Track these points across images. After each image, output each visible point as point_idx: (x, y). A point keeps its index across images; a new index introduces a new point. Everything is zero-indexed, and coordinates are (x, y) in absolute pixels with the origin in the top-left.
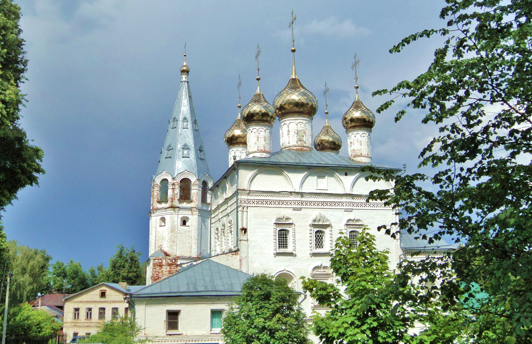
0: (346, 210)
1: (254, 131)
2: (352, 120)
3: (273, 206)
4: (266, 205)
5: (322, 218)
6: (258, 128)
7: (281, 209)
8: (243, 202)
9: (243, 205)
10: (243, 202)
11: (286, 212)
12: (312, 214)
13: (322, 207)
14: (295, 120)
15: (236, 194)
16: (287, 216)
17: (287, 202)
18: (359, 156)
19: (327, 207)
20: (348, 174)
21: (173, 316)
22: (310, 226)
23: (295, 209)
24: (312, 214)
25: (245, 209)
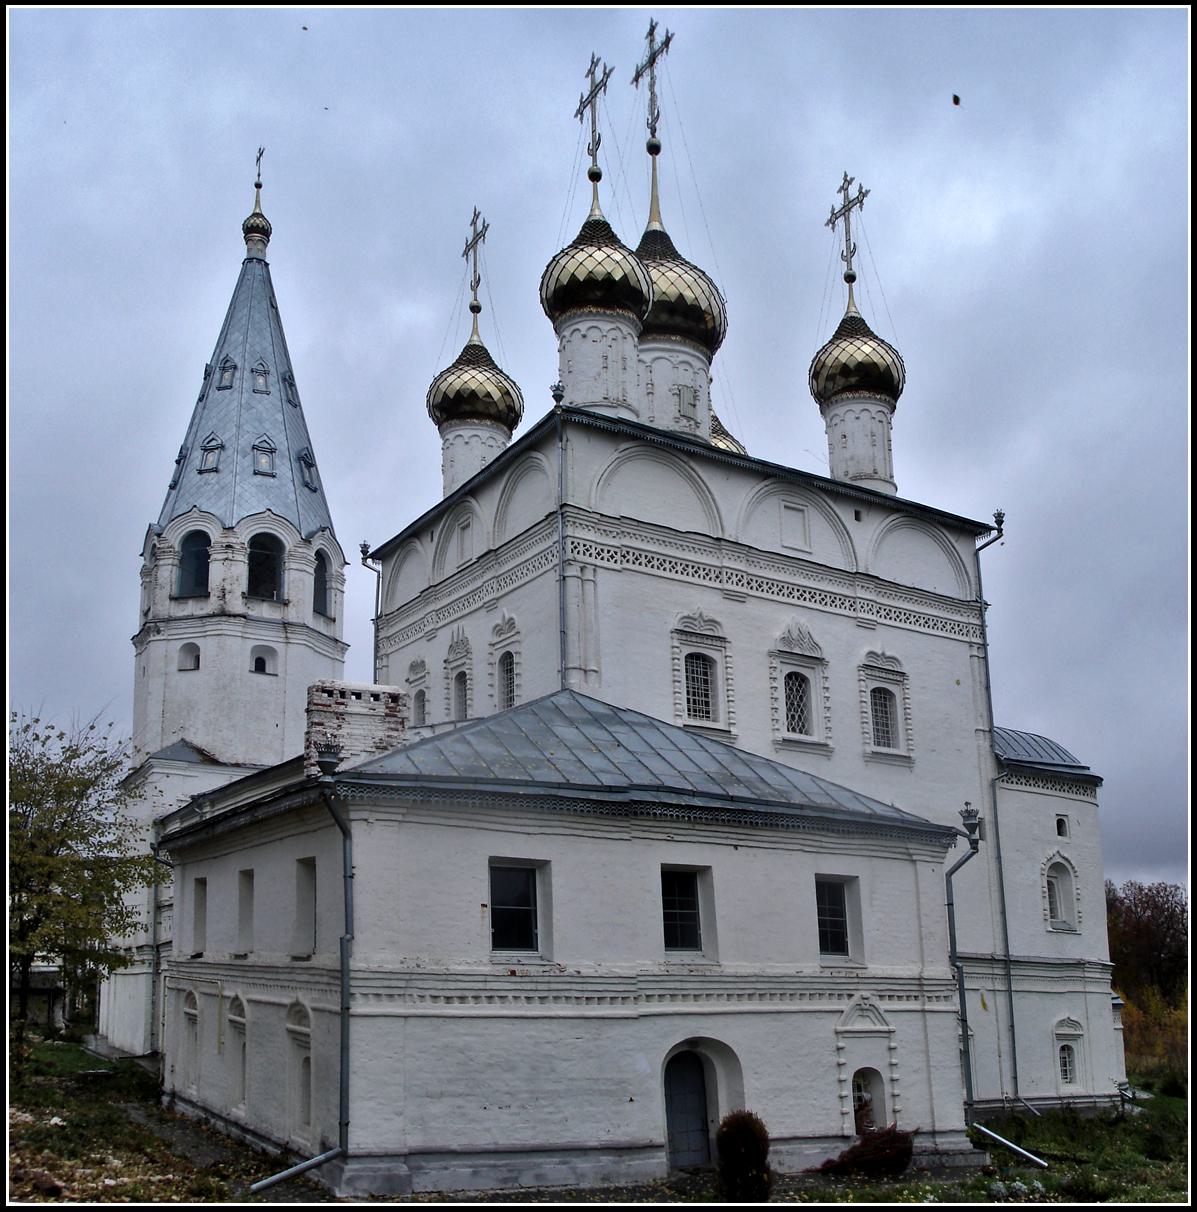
0: (864, 624)
1: (594, 334)
2: (845, 370)
3: (667, 574)
4: (648, 570)
5: (805, 637)
6: (606, 326)
7: (692, 591)
8: (581, 548)
9: (580, 557)
10: (581, 548)
11: (705, 602)
12: (780, 620)
13: (801, 602)
14: (669, 350)
15: (562, 512)
16: (709, 614)
17: (706, 571)
18: (870, 478)
19: (811, 605)
20: (864, 515)
21: (682, 890)
22: (771, 654)
23: (729, 596)
24: (780, 620)
25: (589, 574)
